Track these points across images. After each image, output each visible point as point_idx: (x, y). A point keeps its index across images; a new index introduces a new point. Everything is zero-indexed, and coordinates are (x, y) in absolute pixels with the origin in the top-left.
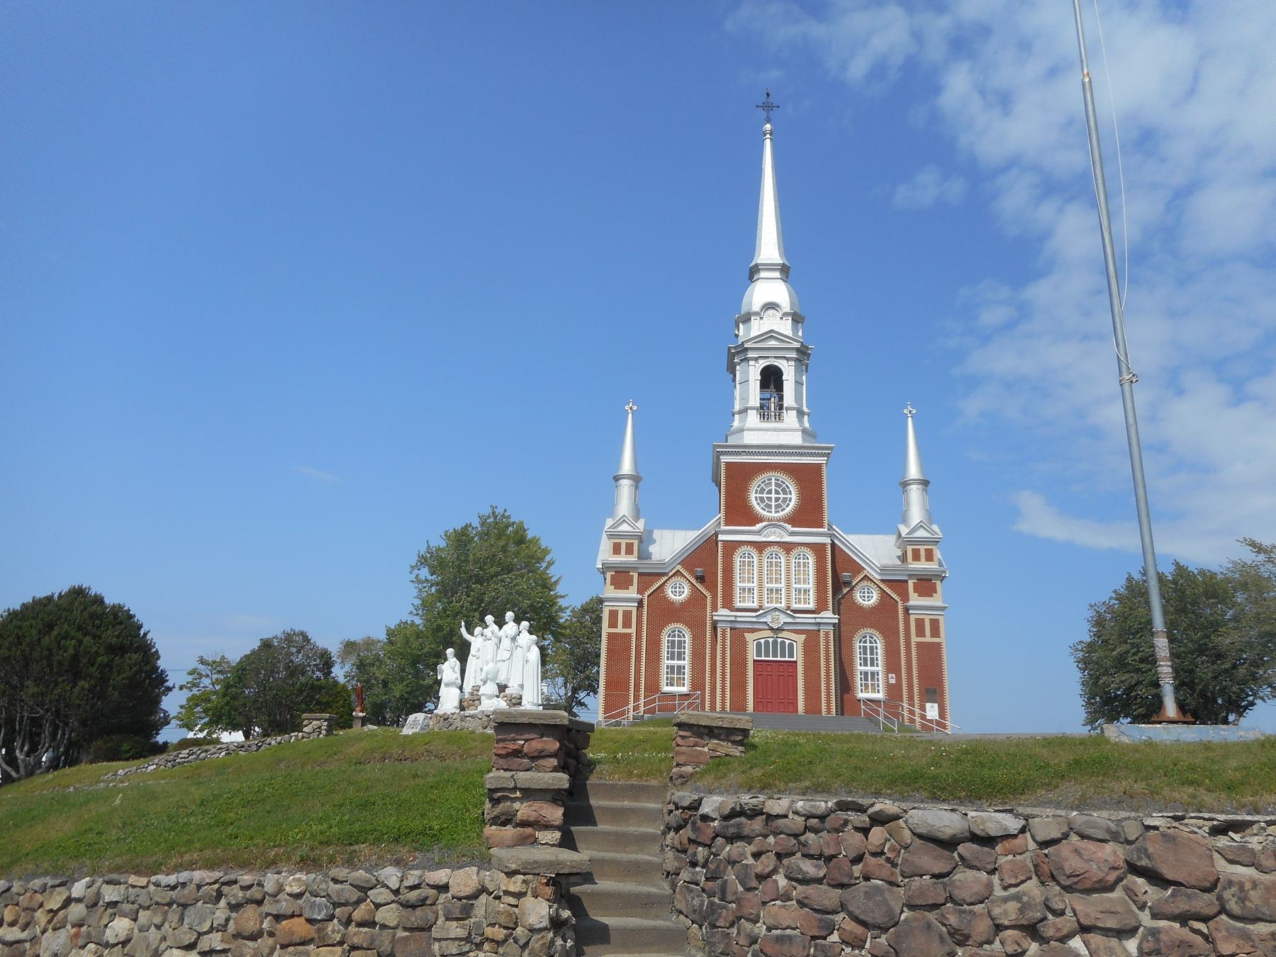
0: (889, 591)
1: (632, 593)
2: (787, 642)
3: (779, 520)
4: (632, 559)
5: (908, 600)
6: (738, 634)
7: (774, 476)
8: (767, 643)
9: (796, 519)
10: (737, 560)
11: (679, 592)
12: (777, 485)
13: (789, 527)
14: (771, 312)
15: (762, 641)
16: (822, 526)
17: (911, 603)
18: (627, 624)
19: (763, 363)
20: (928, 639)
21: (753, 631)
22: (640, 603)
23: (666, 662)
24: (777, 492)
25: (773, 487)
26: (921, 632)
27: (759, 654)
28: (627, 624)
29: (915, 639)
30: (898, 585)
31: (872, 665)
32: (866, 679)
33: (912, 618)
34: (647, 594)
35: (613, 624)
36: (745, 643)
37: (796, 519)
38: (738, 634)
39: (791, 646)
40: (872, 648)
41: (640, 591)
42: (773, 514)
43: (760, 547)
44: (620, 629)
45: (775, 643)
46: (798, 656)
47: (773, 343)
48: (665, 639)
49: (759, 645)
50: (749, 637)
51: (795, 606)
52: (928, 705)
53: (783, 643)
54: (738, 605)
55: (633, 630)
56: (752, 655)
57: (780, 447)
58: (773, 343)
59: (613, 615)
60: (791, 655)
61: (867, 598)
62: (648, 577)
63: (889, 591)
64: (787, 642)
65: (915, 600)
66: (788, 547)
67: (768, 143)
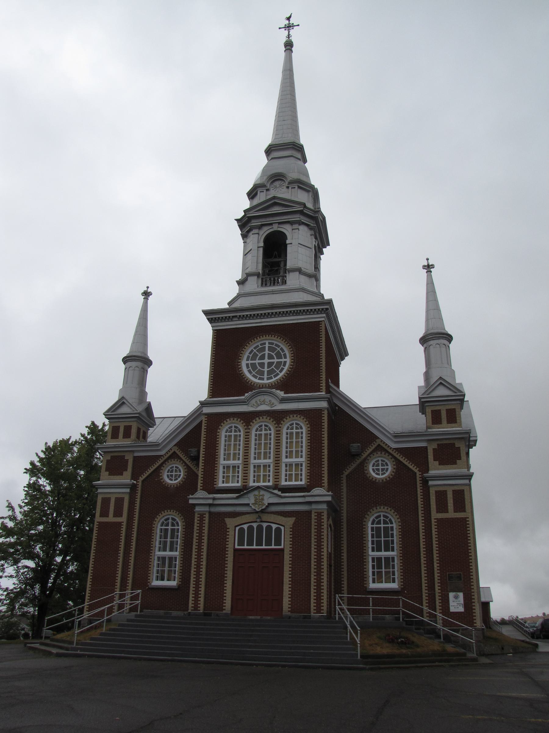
1: (126, 479)
2: (274, 526)
3: (271, 386)
4: (127, 442)
5: (427, 470)
6: (218, 521)
7: (267, 342)
8: (251, 528)
9: (287, 385)
10: (223, 434)
11: (173, 476)
12: (270, 349)
13: (281, 394)
14: (277, 183)
15: (245, 527)
16: (319, 390)
17: (432, 472)
18: (118, 513)
19: (265, 231)
20: (451, 514)
22: (133, 488)
24: (270, 357)
25: (267, 352)
26: (442, 507)
27: (241, 543)
28: (118, 513)
29: (435, 515)
30: (418, 455)
32: (380, 567)
33: (432, 491)
34: (141, 479)
35: (105, 513)
36: (224, 530)
37: (287, 385)
38: (218, 521)
39: (278, 531)
41: (134, 476)
42: (266, 381)
43: (248, 418)
44: (111, 518)
45: (260, 528)
46: (286, 544)
47: (276, 209)
48: (158, 528)
49: (242, 531)
50: (230, 522)
51: (283, 483)
53: (269, 528)
54: (221, 485)
55: (123, 519)
56: (233, 543)
58: (276, 209)
59: (106, 501)
60: (278, 543)
61: (379, 470)
62: (141, 463)
64: (274, 526)
65: (436, 470)
66: (278, 417)
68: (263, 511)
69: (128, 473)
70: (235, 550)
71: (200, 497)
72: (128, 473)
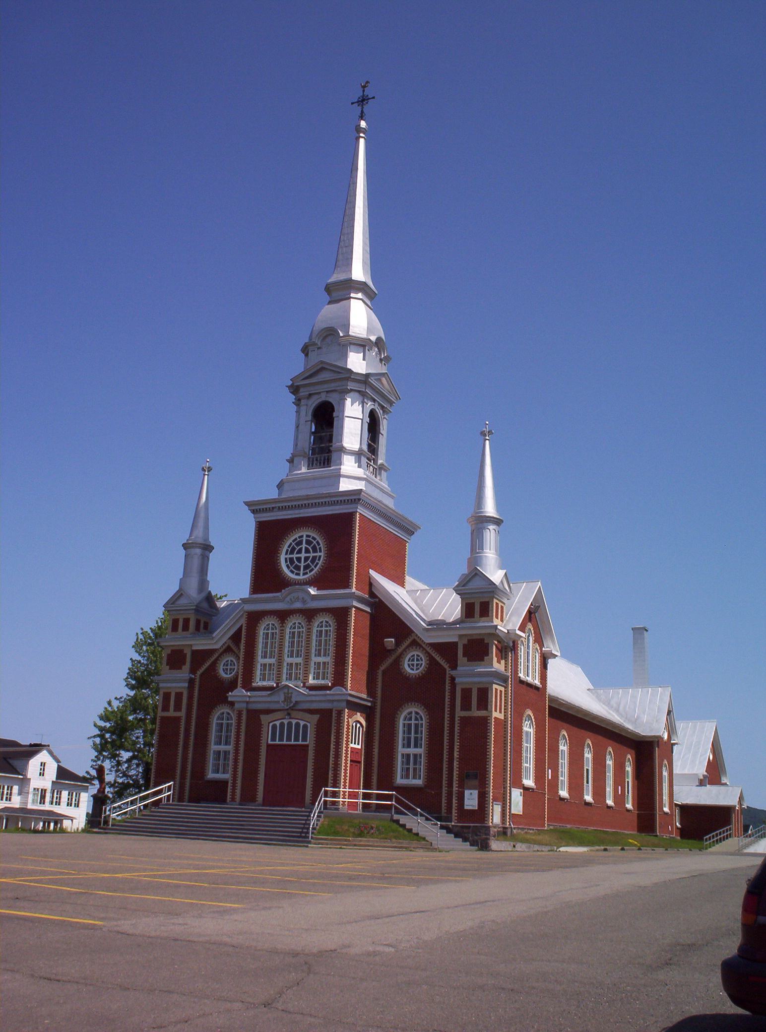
0: (438, 658)
1: (184, 673)
2: (302, 723)
6: (254, 717)
7: (304, 533)
8: (282, 725)
9: (319, 582)
10: (261, 632)
15: (278, 723)
18: (178, 708)
19: (314, 402)
20: (476, 713)
21: (268, 712)
22: (191, 682)
23: (213, 747)
26: (466, 706)
27: (273, 739)
28: (178, 708)
29: (459, 713)
30: (447, 650)
31: (416, 746)
36: (259, 725)
39: (305, 727)
40: (416, 726)
41: (193, 671)
42: (301, 577)
43: (283, 616)
44: (172, 713)
45: (290, 724)
46: (310, 741)
48: (214, 722)
49: (274, 727)
50: (264, 718)
52: (467, 792)
53: (298, 725)
54: (258, 682)
55: (182, 714)
56: (267, 738)
57: (308, 497)
60: (304, 739)
61: (413, 665)
62: (200, 656)
63: (438, 658)
64: (302, 723)
66: (310, 614)
67: (362, 141)
68: (292, 708)
69: (187, 667)
70: (268, 746)
71: (239, 694)
72: (187, 667)
